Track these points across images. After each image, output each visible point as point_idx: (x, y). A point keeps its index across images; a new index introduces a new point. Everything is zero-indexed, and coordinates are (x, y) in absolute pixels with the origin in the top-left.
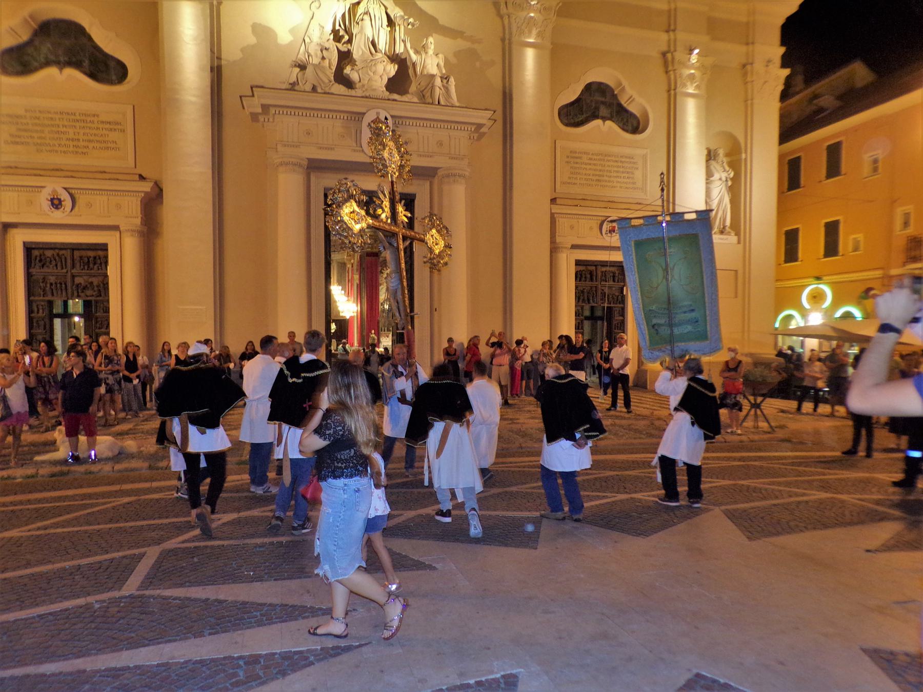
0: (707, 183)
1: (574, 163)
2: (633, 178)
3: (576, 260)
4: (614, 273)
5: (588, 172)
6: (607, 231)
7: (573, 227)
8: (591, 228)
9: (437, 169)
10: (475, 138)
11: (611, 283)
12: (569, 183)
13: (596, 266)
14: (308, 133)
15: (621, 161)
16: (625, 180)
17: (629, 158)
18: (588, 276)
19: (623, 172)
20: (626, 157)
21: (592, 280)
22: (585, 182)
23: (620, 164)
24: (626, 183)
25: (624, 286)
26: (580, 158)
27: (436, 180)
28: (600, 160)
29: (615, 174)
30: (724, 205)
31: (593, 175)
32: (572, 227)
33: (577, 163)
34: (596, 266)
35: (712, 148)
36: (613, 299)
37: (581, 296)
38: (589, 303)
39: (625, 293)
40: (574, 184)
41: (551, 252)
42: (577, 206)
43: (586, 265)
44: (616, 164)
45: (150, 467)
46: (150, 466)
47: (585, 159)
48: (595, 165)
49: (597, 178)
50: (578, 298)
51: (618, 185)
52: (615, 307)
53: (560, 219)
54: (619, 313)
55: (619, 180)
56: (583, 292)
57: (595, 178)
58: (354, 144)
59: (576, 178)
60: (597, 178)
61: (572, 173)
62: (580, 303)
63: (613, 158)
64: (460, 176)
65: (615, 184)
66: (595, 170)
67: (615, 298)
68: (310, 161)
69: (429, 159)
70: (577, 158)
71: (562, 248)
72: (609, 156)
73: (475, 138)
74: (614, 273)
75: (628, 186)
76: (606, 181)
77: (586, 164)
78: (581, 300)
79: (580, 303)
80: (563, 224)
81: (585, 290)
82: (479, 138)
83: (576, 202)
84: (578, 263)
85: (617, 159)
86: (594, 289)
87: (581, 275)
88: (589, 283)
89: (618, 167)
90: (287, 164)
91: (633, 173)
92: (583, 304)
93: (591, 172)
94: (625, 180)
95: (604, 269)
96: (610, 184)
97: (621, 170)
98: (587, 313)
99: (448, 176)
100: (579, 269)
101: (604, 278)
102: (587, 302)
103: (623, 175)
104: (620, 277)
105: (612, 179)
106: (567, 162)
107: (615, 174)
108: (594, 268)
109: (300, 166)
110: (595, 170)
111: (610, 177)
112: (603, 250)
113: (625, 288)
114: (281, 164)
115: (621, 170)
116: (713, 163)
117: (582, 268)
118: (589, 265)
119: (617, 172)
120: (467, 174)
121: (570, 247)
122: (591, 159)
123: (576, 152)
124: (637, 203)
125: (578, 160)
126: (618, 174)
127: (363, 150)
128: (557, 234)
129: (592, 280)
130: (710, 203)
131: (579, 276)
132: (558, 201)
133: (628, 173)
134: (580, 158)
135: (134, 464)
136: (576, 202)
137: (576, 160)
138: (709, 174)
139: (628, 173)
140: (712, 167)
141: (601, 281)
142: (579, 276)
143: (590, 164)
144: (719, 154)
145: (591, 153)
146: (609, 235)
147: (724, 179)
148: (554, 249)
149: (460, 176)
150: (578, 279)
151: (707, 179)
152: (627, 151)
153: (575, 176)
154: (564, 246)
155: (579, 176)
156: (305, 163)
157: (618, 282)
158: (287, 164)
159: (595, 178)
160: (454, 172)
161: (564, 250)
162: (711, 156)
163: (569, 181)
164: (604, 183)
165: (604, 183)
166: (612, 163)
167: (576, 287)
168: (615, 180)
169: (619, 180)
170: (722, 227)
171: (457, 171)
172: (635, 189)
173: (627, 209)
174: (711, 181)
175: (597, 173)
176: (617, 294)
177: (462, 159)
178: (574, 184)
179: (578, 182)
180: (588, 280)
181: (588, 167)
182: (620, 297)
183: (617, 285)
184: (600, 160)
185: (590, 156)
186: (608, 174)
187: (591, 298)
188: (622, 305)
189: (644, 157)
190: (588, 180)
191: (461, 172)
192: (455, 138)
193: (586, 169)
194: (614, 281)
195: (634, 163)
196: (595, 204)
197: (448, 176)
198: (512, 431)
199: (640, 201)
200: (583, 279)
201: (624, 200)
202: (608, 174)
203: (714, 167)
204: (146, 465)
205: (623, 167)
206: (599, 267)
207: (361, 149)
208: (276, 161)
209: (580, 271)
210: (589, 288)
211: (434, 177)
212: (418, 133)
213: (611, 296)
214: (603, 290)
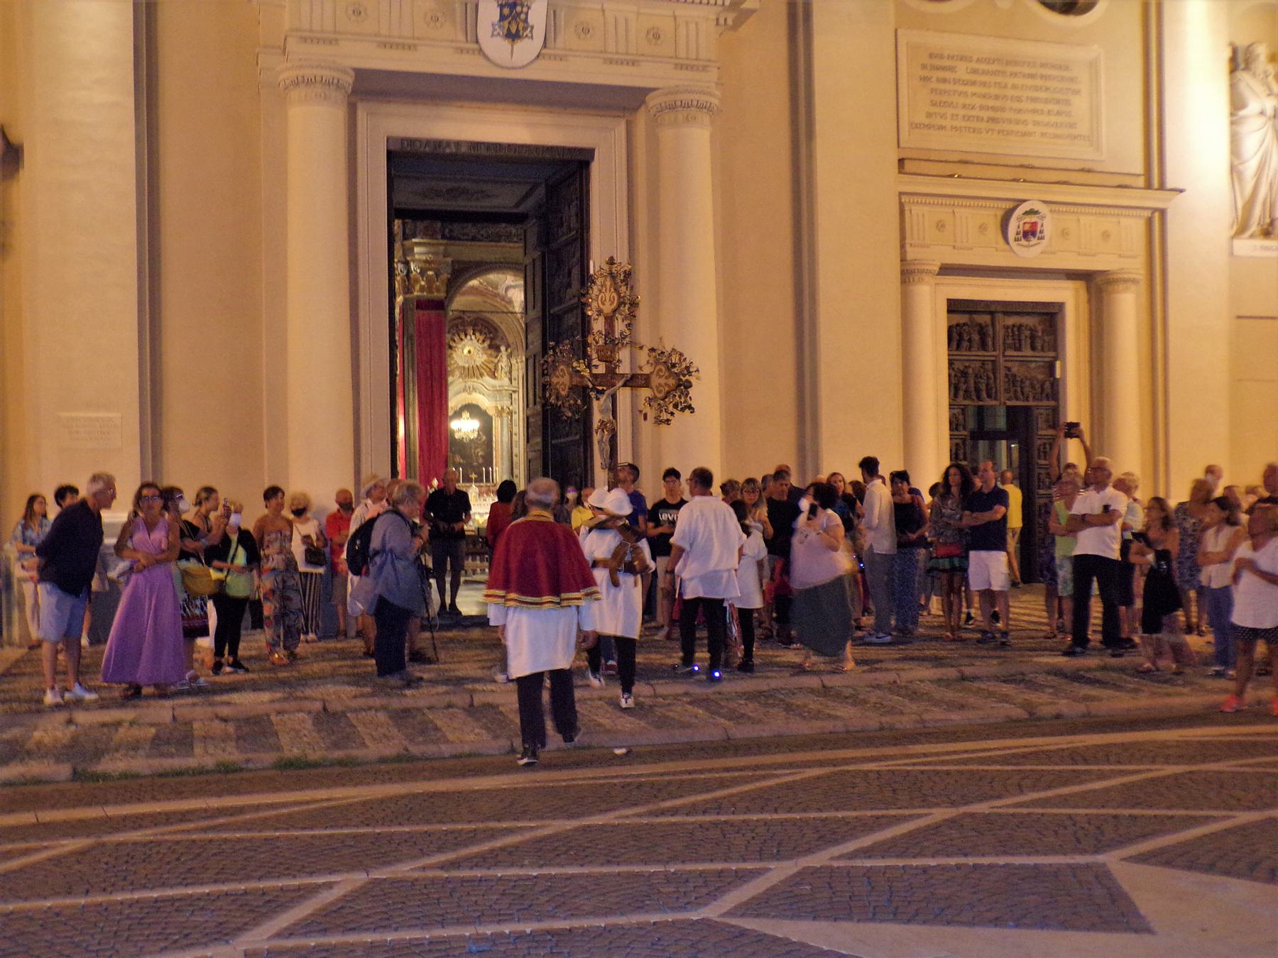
0: (1232, 123)
1: (938, 80)
2: (1069, 114)
3: (949, 301)
4: (1033, 330)
5: (968, 101)
6: (1018, 233)
7: (943, 226)
8: (982, 228)
9: (645, 91)
10: (730, 22)
11: (1030, 353)
12: (928, 126)
13: (992, 313)
14: (357, 13)
15: (1042, 77)
16: (1053, 119)
17: (1060, 67)
18: (976, 337)
19: (1047, 101)
20: (1054, 67)
21: (983, 346)
22: (963, 124)
23: (1039, 82)
24: (1056, 125)
25: (1056, 358)
26: (951, 69)
27: (641, 119)
28: (995, 73)
29: (1031, 106)
30: (1271, 174)
31: (982, 108)
32: (940, 226)
33: (944, 81)
34: (992, 313)
35: (1242, 42)
36: (1033, 387)
37: (959, 382)
38: (979, 398)
39: (1058, 375)
40: (942, 128)
41: (903, 282)
42: (951, 176)
43: (970, 312)
44: (1030, 82)
45: (76, 775)
46: (75, 772)
47: (962, 71)
48: (984, 84)
49: (991, 114)
50: (955, 389)
51: (1038, 129)
52: (1038, 407)
53: (916, 209)
54: (1047, 421)
55: (1045, 118)
56: (964, 374)
57: (985, 114)
58: (461, 37)
59: (943, 116)
60: (991, 114)
61: (934, 104)
62: (961, 401)
63: (1027, 70)
64: (700, 107)
65: (1030, 128)
66: (984, 96)
67: (1038, 386)
68: (360, 74)
69: (630, 69)
70: (943, 68)
71: (922, 271)
72: (1016, 63)
73: (730, 22)
74: (1033, 330)
75: (1058, 131)
76: (1010, 121)
77: (966, 83)
78: (961, 393)
79: (961, 401)
80: (920, 215)
81: (970, 371)
82: (736, 26)
83: (948, 169)
84: (954, 307)
85: (1033, 71)
86: (989, 366)
87: (960, 335)
88: (977, 354)
89: (1036, 88)
90: (309, 82)
91: (1067, 102)
92: (967, 402)
93: (978, 101)
94: (1053, 119)
95: (1011, 321)
96: (1020, 128)
97: (1043, 95)
98: (972, 424)
99: (672, 107)
100: (954, 323)
101: (1010, 341)
102: (974, 397)
103: (1047, 107)
104: (1046, 338)
105: (1022, 117)
106: (925, 79)
107: (1031, 106)
108: (985, 319)
109: (339, 86)
110: (984, 96)
111: (1020, 111)
112: (1009, 277)
113: (1058, 364)
114: (296, 83)
115: (1043, 95)
116: (1243, 76)
117: (962, 319)
118: (976, 312)
119: (1034, 100)
120: (715, 101)
121: (937, 269)
122: (975, 71)
123: (941, 57)
124: (1082, 170)
125: (947, 75)
126: (1039, 106)
127: (481, 50)
128: (908, 241)
129: (983, 346)
130: (1241, 167)
131: (956, 337)
132: (908, 166)
133: (1058, 102)
134: (951, 69)
135: (35, 768)
136: (948, 169)
137: (941, 74)
138: (1237, 104)
139: (1058, 102)
140: (1243, 87)
141: (1005, 350)
142: (956, 336)
143: (974, 83)
144: (1258, 56)
145: (975, 58)
146: (1023, 242)
147: (1270, 112)
148: (907, 274)
149: (700, 107)
150: (955, 346)
151: (1232, 114)
152: (1052, 52)
153: (943, 110)
154: (926, 267)
155: (950, 111)
156: (349, 80)
157: (1043, 350)
158: (309, 82)
159: (985, 114)
160: (686, 97)
161: (926, 278)
162: (1238, 62)
163: (927, 121)
164: (1006, 127)
165: (1006, 127)
166: (1019, 81)
167: (951, 363)
168: (1029, 117)
169: (1038, 118)
170: (1268, 220)
171: (695, 97)
172: (1075, 137)
173: (1065, 183)
174: (1245, 117)
175: (991, 103)
176: (1040, 377)
177: (705, 68)
178: (942, 128)
179: (948, 123)
180: (975, 345)
181: (970, 89)
182: (1047, 384)
183: (1040, 357)
184: (995, 73)
185: (974, 65)
186: (1016, 105)
187: (983, 387)
188: (1052, 403)
189: (1093, 65)
190: (969, 118)
191: (703, 98)
192: (687, 23)
193: (965, 94)
194: (1033, 348)
195: (1072, 80)
196: (990, 172)
197: (672, 107)
198: (878, 687)
199: (1087, 166)
200: (965, 344)
201: (1050, 164)
202: (1016, 105)
203: (1248, 85)
204: (64, 770)
205: (1047, 89)
206: (999, 317)
207: (475, 46)
208: (281, 77)
209: (958, 325)
210: (978, 364)
211: (636, 109)
212: (604, 11)
213: (1027, 383)
214: (1009, 369)
